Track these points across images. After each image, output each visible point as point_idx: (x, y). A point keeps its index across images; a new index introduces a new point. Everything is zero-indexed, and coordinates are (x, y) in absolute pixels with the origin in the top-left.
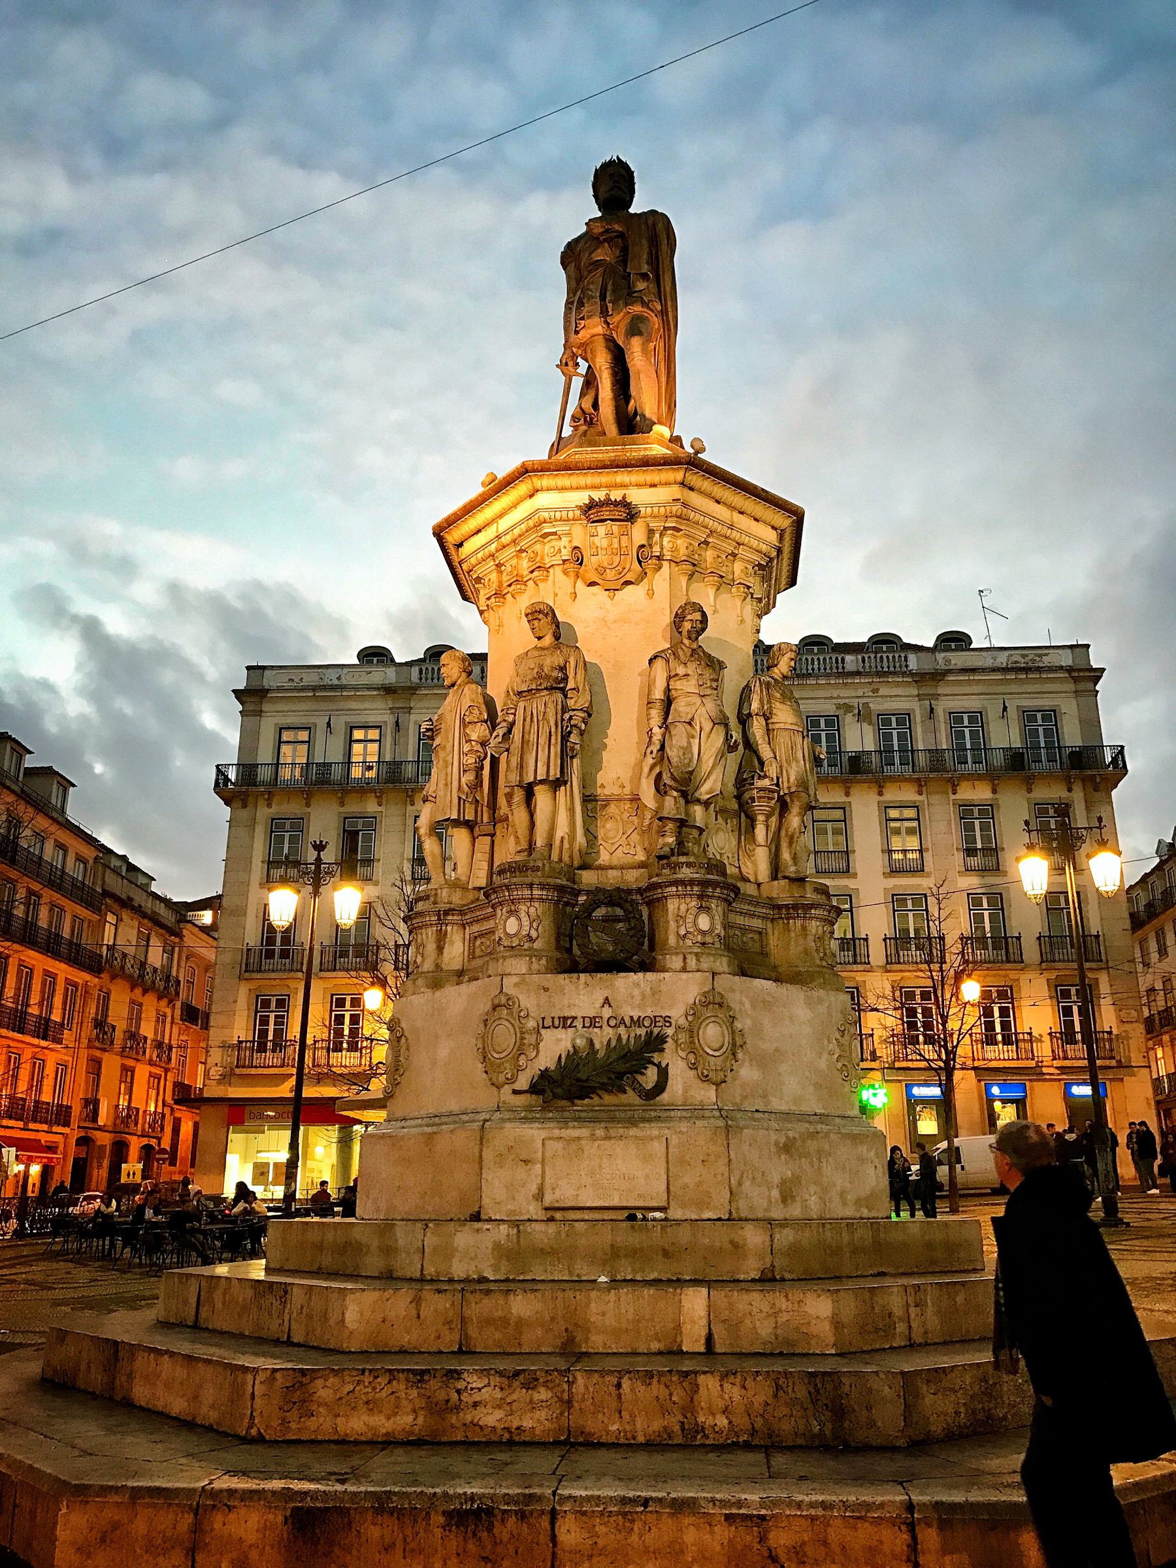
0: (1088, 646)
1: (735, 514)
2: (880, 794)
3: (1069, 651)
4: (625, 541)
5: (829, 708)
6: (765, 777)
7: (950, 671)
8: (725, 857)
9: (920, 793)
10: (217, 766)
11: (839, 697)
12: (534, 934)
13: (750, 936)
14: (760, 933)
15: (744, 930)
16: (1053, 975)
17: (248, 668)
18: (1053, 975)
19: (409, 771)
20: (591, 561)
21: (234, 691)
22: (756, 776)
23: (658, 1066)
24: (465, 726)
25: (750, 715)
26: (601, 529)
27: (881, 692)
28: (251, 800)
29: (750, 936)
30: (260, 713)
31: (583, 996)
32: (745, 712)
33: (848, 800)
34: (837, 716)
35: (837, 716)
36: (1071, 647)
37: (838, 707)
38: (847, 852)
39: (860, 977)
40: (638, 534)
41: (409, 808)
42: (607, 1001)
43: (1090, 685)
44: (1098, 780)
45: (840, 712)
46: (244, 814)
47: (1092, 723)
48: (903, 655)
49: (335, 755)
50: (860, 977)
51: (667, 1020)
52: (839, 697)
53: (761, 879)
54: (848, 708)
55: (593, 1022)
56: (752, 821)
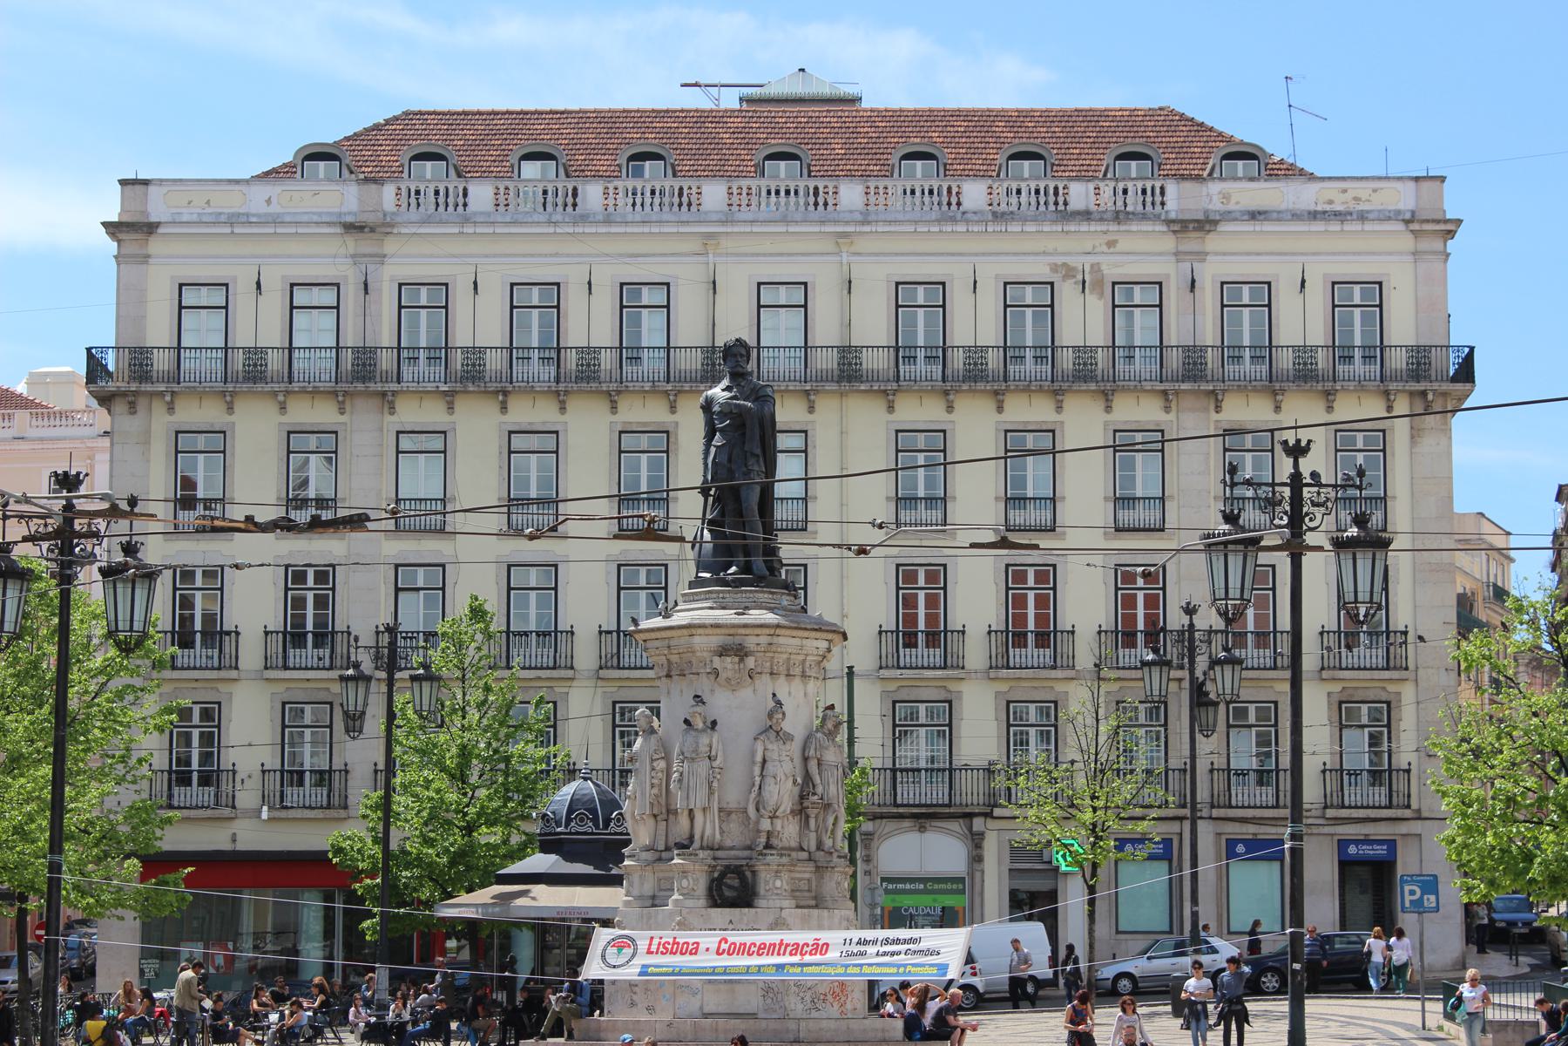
0: (1442, 179)
2: (1108, 409)
3: (1412, 184)
5: (1038, 269)
7: (1228, 216)
9: (1167, 409)
10: (89, 350)
11: (1055, 253)
15: (800, 880)
16: (1336, 688)
17: (123, 183)
18: (1336, 688)
19: (386, 361)
20: (723, 675)
21: (103, 224)
24: (652, 760)
26: (729, 659)
27: (1120, 247)
28: (142, 403)
30: (145, 258)
33: (1057, 418)
36: (1417, 179)
37: (1055, 268)
38: (1053, 500)
39: (1060, 687)
40: (750, 662)
41: (388, 418)
43: (1437, 245)
44: (1430, 397)
46: (130, 424)
47: (1434, 308)
48: (1158, 185)
49: (272, 337)
50: (1060, 687)
52: (1055, 253)
54: (1069, 272)
56: (808, 817)
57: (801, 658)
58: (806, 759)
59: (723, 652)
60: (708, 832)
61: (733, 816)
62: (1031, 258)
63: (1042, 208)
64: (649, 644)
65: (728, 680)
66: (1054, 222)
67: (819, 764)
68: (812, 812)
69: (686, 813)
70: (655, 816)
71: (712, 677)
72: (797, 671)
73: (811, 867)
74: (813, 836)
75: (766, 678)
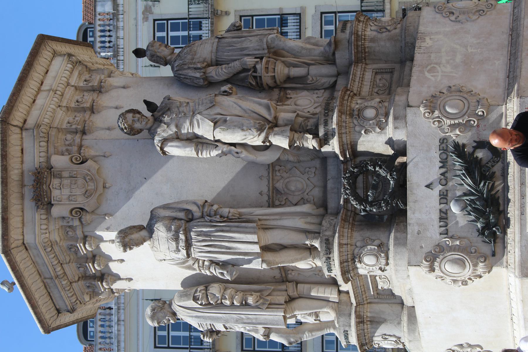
1: (44, 88)
4: (65, 174)
6: (255, 67)
8: (317, 100)
12: (377, 242)
13: (378, 81)
14: (376, 73)
20: (81, 201)
22: (254, 74)
23: (475, 148)
25: (205, 79)
26: (55, 193)
29: (378, 81)
31: (423, 205)
32: (201, 82)
34: (155, 20)
35: (155, 20)
39: (396, 7)
40: (59, 161)
42: (428, 186)
45: (151, 18)
51: (443, 141)
52: (136, 19)
53: (335, 72)
54: (147, 10)
55: (444, 197)
56: (289, 79)
57: (69, 92)
58: (210, 84)
59: (43, 202)
60: (300, 223)
61: (279, 185)
62: (139, 34)
63: (111, 28)
64: (60, 305)
65: (87, 194)
66: (118, 20)
67: (218, 63)
68: (281, 70)
69: (269, 256)
70: (291, 300)
71: (87, 218)
72: (88, 98)
73: (357, 71)
74: (314, 70)
75: (88, 140)
